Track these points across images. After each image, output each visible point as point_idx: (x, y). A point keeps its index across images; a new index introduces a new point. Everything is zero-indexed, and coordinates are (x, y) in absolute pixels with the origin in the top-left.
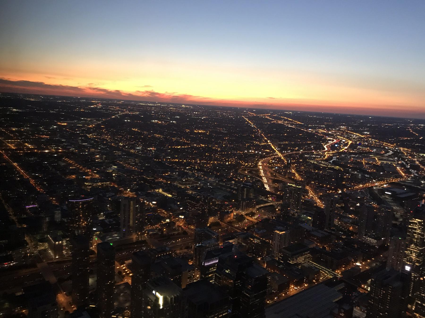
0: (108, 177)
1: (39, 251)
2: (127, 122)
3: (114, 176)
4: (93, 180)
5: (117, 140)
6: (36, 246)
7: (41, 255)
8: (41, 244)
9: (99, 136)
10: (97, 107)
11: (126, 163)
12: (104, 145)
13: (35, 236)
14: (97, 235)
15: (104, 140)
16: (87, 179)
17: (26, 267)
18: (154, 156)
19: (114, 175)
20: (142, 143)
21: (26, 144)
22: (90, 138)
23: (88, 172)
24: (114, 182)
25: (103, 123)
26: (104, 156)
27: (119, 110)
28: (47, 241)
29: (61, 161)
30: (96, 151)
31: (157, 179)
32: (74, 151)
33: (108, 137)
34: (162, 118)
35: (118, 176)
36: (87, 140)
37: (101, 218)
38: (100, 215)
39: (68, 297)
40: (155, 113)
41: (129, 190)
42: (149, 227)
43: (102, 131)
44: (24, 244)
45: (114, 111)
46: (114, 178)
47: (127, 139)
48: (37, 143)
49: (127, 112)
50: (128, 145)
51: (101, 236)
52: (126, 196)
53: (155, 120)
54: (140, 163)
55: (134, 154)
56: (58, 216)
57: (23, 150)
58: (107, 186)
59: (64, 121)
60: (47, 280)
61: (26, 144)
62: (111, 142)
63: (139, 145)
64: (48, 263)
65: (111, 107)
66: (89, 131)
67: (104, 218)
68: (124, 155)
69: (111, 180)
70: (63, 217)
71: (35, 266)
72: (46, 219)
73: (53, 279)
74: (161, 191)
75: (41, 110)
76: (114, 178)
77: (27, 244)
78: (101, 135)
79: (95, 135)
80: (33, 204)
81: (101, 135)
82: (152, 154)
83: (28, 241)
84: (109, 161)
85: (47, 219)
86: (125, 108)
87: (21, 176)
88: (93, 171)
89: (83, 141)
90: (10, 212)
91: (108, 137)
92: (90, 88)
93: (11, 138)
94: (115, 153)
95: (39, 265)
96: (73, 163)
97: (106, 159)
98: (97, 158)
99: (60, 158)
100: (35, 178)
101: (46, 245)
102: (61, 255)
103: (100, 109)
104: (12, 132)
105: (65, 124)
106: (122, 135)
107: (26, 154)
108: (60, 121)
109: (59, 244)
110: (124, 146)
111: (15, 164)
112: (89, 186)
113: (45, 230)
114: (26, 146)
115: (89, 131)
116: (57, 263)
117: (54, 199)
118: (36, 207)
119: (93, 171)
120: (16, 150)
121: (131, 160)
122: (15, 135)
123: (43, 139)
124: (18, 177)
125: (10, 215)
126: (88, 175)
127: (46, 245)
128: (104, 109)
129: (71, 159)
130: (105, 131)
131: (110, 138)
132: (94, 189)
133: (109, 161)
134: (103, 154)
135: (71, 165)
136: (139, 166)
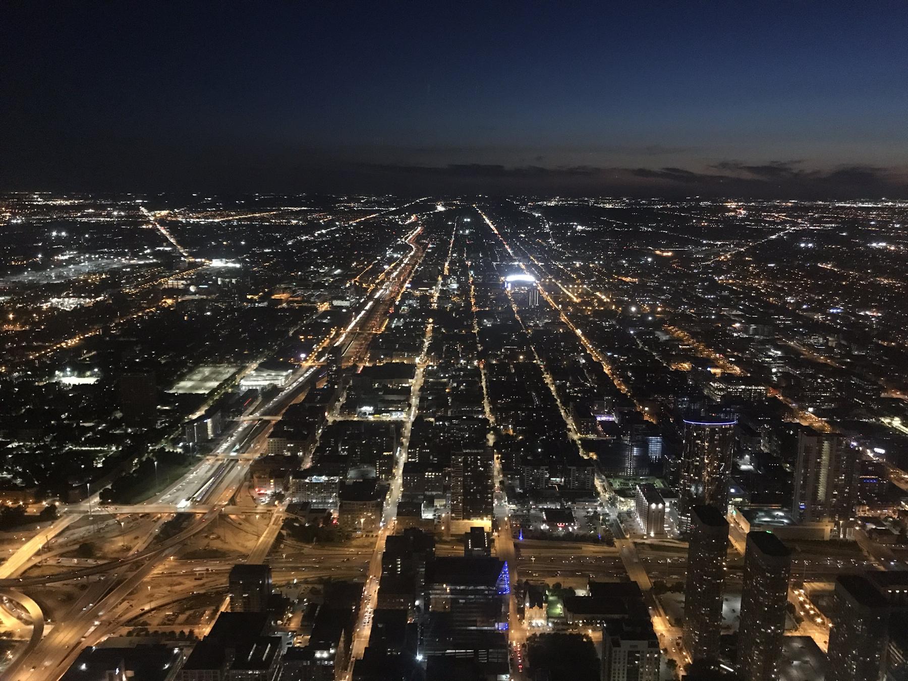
0: (759, 374)
1: (620, 515)
2: (807, 248)
3: (775, 373)
4: (727, 378)
5: (782, 290)
6: (612, 502)
7: (622, 523)
8: (622, 499)
9: (741, 279)
10: (735, 217)
11: (804, 345)
12: (752, 300)
13: (611, 481)
14: (736, 505)
15: (753, 288)
16: (715, 374)
17: (595, 540)
18: (876, 332)
19: (774, 370)
20: (843, 299)
21: (598, 293)
22: (722, 285)
23: (716, 359)
24: (776, 387)
25: (748, 252)
26: (753, 326)
27: (786, 222)
28: (633, 496)
29: (661, 331)
30: (734, 312)
31: (885, 390)
32: (687, 312)
33: (760, 284)
34: (899, 237)
35: (785, 376)
36: (714, 287)
37: (743, 467)
38: (742, 457)
39: (673, 629)
40: (883, 224)
41: (811, 410)
42: (863, 511)
43: (748, 270)
44: (591, 494)
45: (774, 223)
46: (775, 379)
47: (805, 288)
48: (615, 289)
49: (807, 225)
50: (810, 301)
51: (746, 509)
52: (805, 424)
53: (878, 241)
54: (839, 346)
55: (823, 323)
56: (655, 446)
57: (592, 305)
58: (760, 393)
59: (667, 247)
60: (632, 579)
61: (598, 293)
62: (769, 295)
63: (837, 303)
64: (635, 543)
65: (767, 216)
66: (718, 269)
67: (751, 467)
68: (799, 326)
69: (768, 382)
70: (664, 450)
71: (611, 544)
72: (632, 450)
73: (644, 581)
74: (897, 422)
75: (626, 227)
76: (775, 379)
77: (598, 494)
78: (744, 279)
79: (731, 278)
80: (609, 414)
81: (744, 279)
82: (871, 327)
83: (600, 489)
84: (762, 337)
85: (635, 451)
86: (801, 217)
87: (588, 357)
88: (727, 357)
89: (707, 290)
90: (571, 424)
91: (760, 284)
92: (724, 165)
93: (573, 281)
94: (779, 319)
95: (617, 543)
96: (685, 336)
97: (756, 332)
98: (735, 330)
99: (658, 324)
100: (612, 361)
101: (632, 503)
102: (660, 534)
103: (743, 220)
104: (575, 270)
105: (670, 254)
106: (794, 279)
107: (596, 313)
108: (658, 246)
109: (657, 504)
110: (798, 305)
111: (579, 332)
112: (721, 390)
113: (630, 472)
114: (596, 297)
115: (718, 269)
116: (651, 546)
117: (647, 409)
118: (613, 422)
119: (727, 357)
120: (579, 304)
121: (817, 340)
122: (579, 277)
123: (626, 283)
124: (584, 357)
125: (570, 430)
126: (716, 367)
127: (632, 503)
128: (751, 221)
129: (680, 328)
130: (754, 268)
131: (765, 286)
132: (729, 399)
133: (762, 337)
134: (750, 321)
135: (680, 340)
136: (837, 354)
